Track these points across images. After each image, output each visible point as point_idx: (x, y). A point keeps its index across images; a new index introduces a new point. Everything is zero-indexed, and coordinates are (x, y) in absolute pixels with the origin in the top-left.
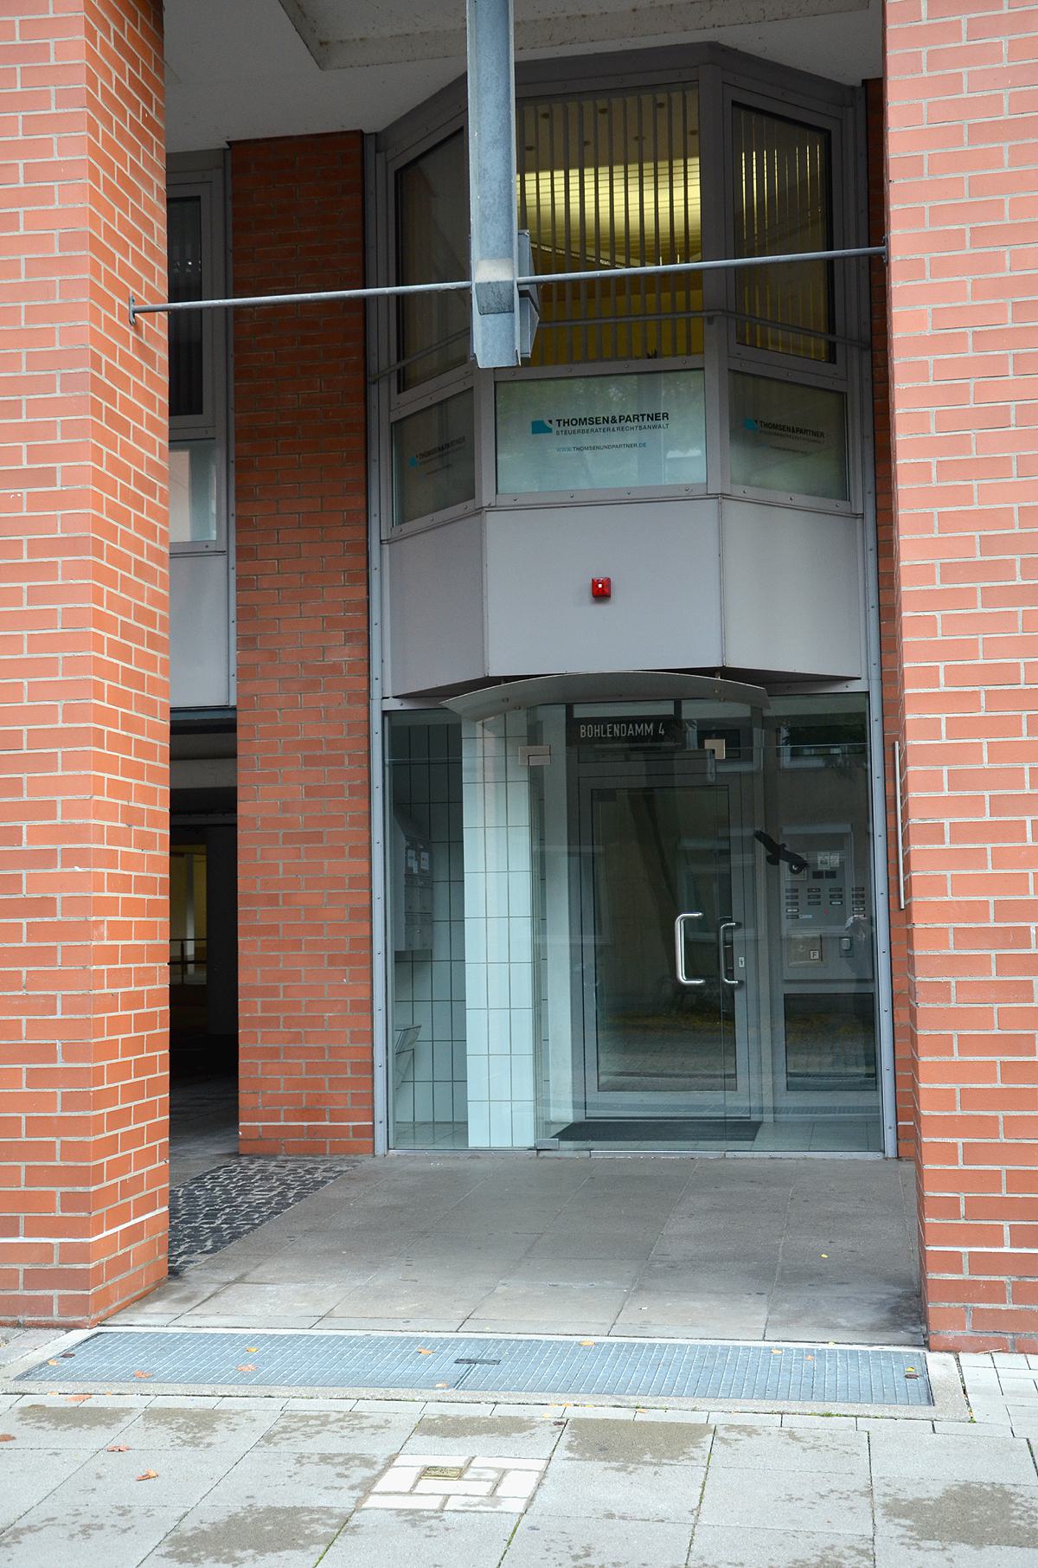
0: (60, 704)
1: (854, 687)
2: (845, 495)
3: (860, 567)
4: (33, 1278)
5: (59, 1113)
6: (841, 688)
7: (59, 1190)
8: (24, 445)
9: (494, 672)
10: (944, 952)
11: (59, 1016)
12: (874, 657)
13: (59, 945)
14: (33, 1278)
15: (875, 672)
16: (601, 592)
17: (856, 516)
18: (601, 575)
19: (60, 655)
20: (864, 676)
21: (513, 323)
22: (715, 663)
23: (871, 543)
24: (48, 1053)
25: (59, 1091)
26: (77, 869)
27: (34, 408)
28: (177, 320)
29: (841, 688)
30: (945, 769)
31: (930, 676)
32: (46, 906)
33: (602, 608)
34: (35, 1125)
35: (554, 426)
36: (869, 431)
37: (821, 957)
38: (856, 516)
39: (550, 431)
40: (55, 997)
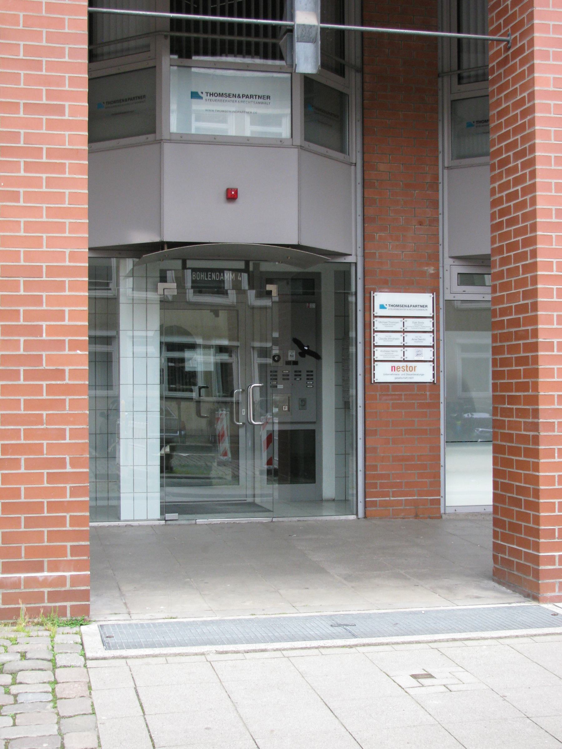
0: (67, 251)
1: (349, 259)
2: (342, 149)
3: (353, 191)
4: (53, 596)
5: (68, 499)
6: (342, 260)
7: (69, 544)
8: (44, 89)
9: (169, 237)
10: (552, 407)
11: (68, 441)
12: (360, 243)
13: (68, 398)
14: (53, 596)
15: (360, 252)
16: (231, 196)
17: (351, 164)
18: (232, 185)
19: (67, 221)
20: (353, 253)
21: (166, 31)
22: (295, 242)
23: (359, 180)
24: (61, 463)
25: (68, 486)
26: (79, 352)
27: (51, 66)
28: (91, 16)
29: (342, 260)
30: (555, 314)
31: (549, 266)
32: (59, 374)
33: (231, 206)
34: (52, 506)
35: (204, 96)
36: (359, 117)
37: (289, 408)
38: (351, 164)
39: (201, 98)
40: (65, 429)
